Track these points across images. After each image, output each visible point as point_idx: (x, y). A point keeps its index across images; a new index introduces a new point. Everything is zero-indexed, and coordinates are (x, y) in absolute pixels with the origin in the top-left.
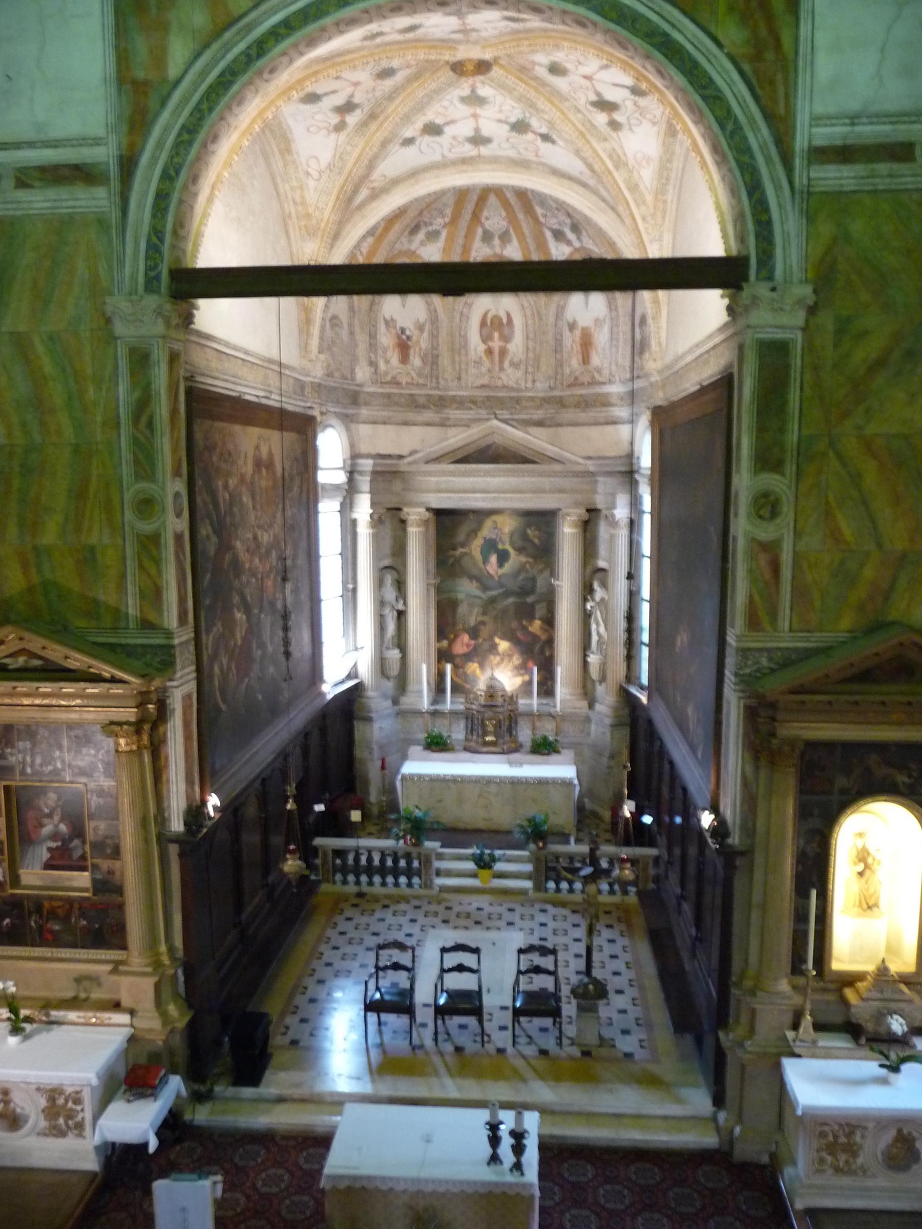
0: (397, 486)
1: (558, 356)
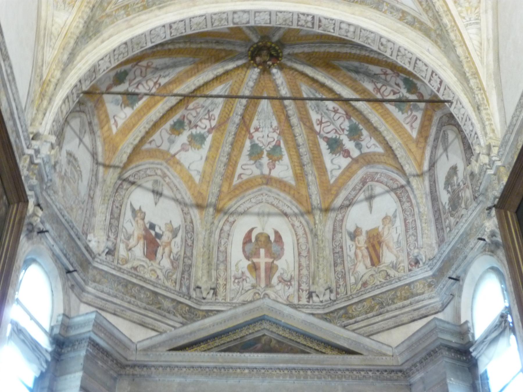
1: (339, 268)
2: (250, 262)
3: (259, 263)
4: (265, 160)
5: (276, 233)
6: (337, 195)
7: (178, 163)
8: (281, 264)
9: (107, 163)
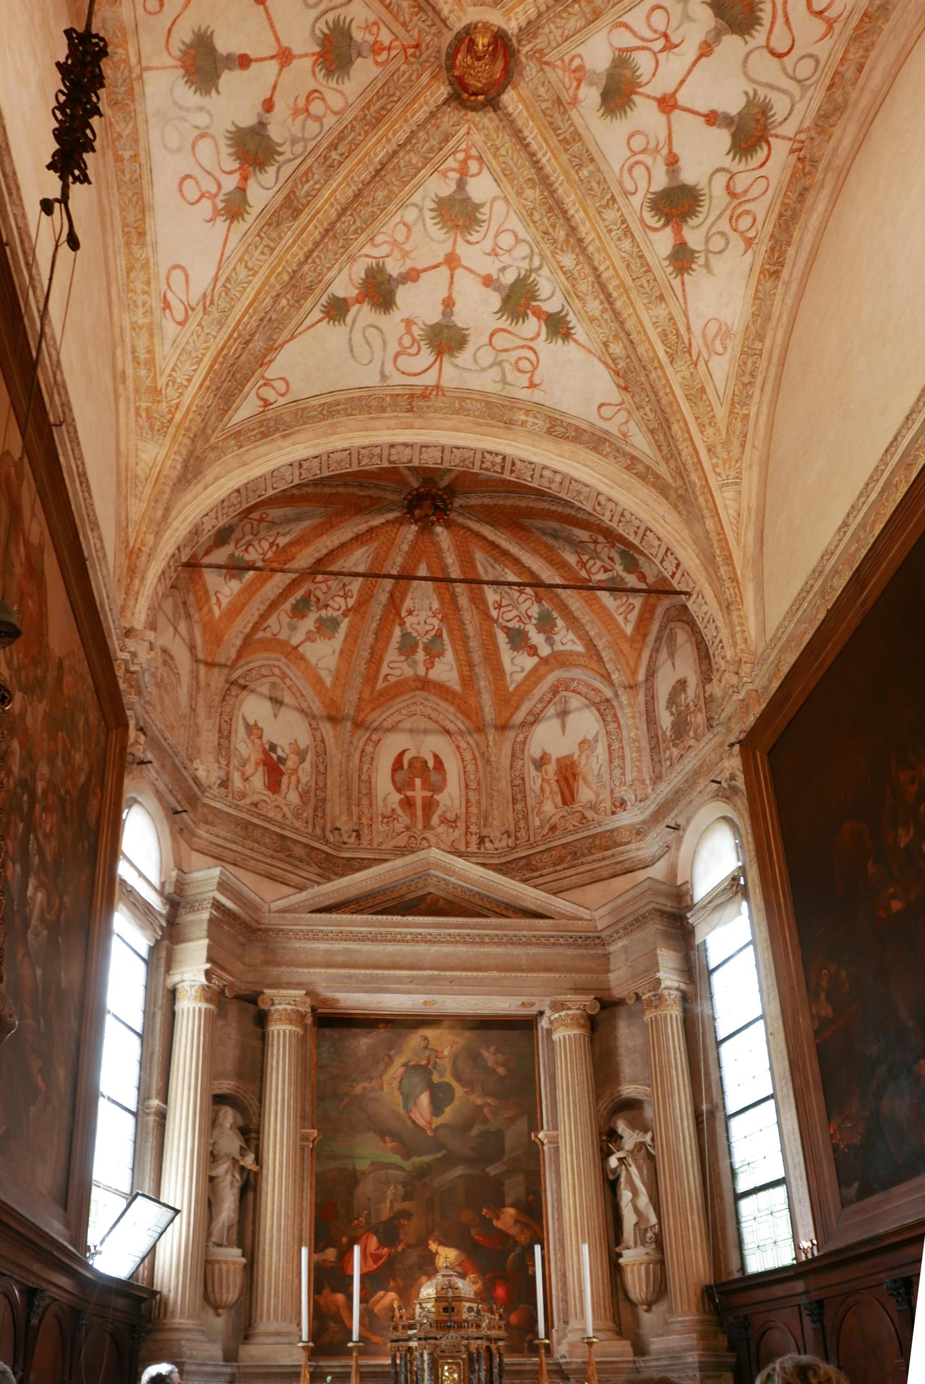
2: (402, 796)
3: (414, 797)
4: (420, 656)
5: (436, 757)
6: (517, 708)
7: (302, 658)
8: (442, 798)
9: (210, 660)
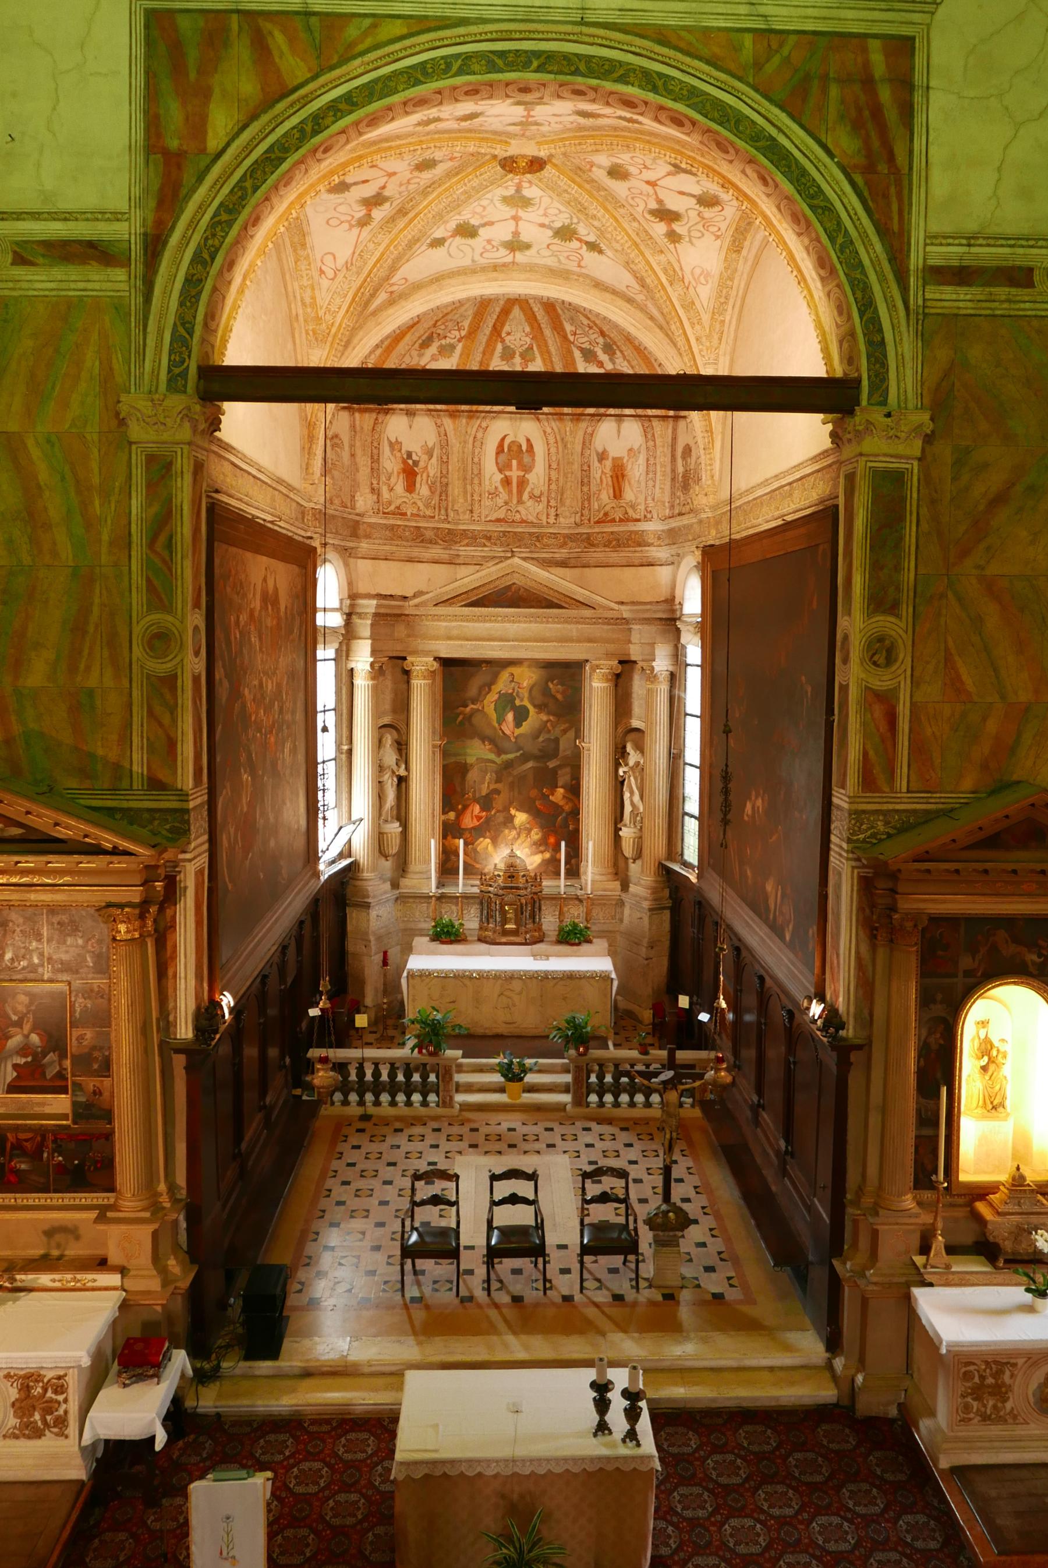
0: (401, 631)
1: (585, 489)
8: (531, 477)
